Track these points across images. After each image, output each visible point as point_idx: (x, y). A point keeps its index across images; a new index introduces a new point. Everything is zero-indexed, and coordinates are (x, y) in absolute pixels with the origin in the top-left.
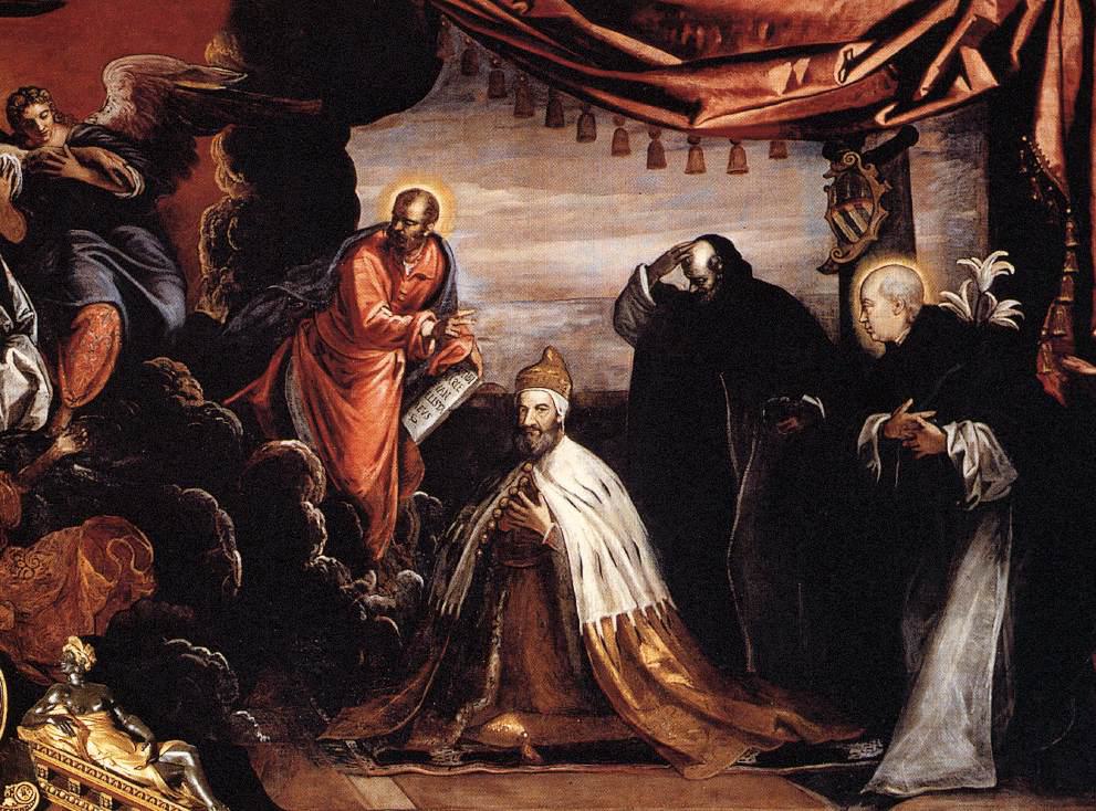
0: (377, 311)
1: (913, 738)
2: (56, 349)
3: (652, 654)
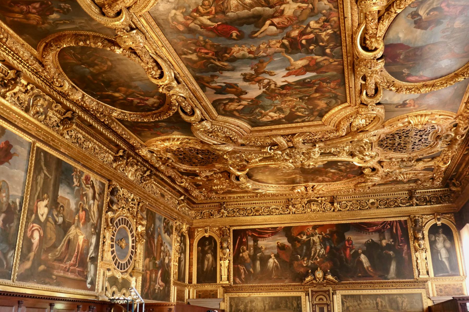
0: (348, 245)
1: (390, 274)
2: (325, 249)
3: (370, 269)
